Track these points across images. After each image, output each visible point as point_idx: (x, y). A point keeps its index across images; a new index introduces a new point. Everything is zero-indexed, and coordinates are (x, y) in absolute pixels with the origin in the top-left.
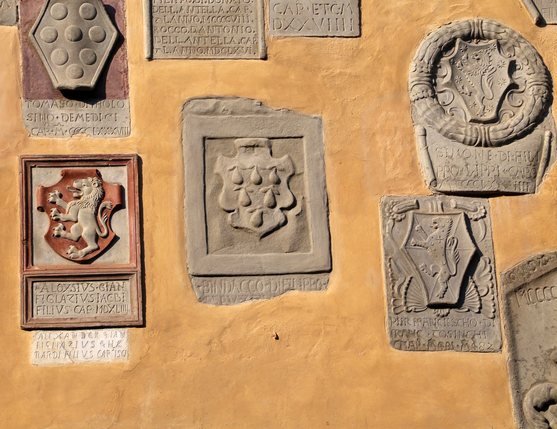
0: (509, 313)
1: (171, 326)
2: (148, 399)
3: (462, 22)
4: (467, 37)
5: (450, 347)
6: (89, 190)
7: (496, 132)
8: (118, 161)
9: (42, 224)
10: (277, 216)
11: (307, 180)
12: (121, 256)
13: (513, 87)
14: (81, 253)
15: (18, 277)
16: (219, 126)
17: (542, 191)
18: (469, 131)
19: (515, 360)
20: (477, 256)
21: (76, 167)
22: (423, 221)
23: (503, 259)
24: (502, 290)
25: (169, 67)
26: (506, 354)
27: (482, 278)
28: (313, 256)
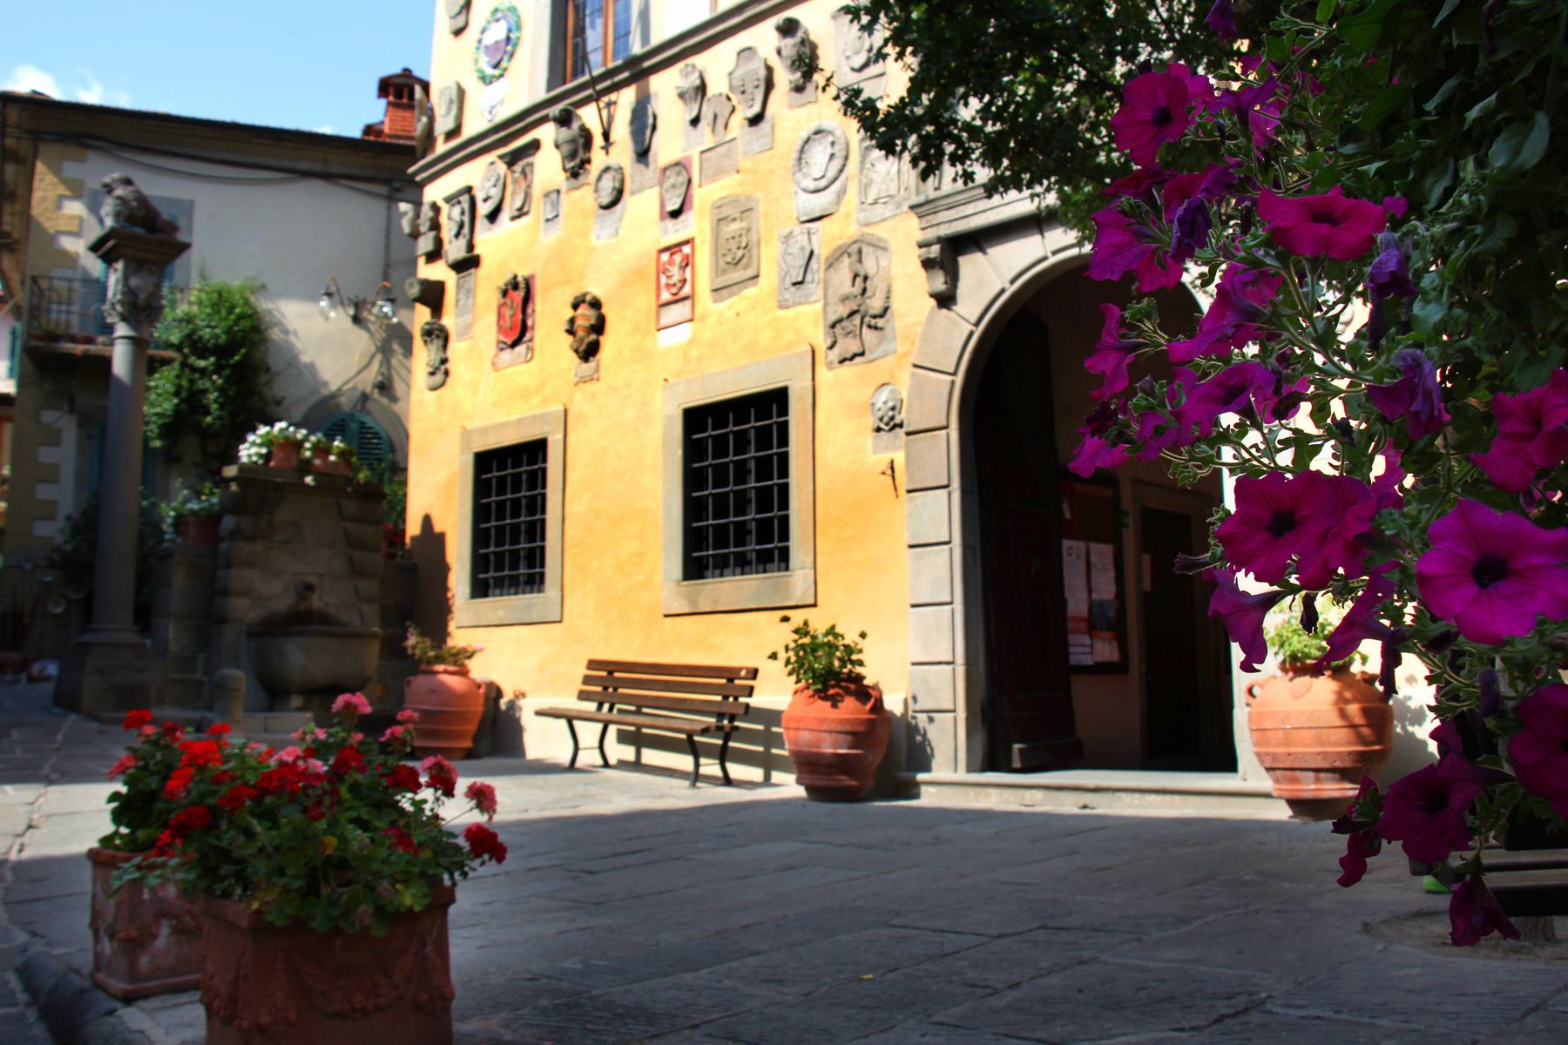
0: (825, 281)
1: (704, 318)
2: (694, 354)
3: (813, 127)
4: (817, 133)
5: (800, 304)
6: (678, 258)
7: (823, 183)
8: (687, 242)
9: (663, 280)
10: (740, 253)
11: (754, 231)
12: (687, 290)
13: (832, 156)
14: (674, 290)
15: (654, 305)
16: (725, 212)
17: (842, 210)
18: (812, 185)
19: (826, 305)
20: (812, 253)
21: (672, 249)
22: (792, 241)
23: (822, 252)
24: (823, 267)
25: (707, 188)
26: (821, 304)
27: (813, 264)
28: (750, 272)
